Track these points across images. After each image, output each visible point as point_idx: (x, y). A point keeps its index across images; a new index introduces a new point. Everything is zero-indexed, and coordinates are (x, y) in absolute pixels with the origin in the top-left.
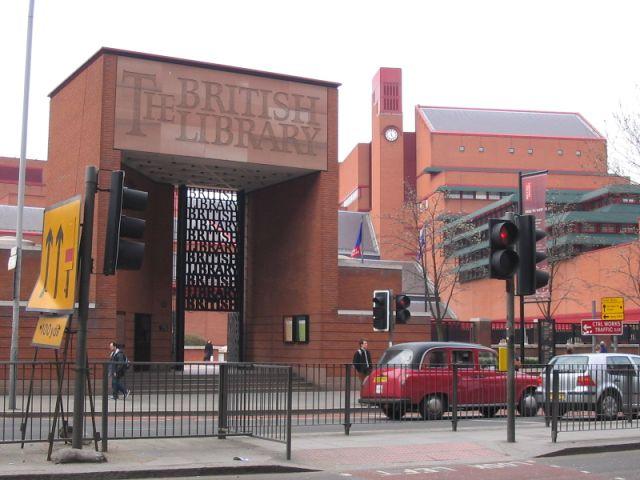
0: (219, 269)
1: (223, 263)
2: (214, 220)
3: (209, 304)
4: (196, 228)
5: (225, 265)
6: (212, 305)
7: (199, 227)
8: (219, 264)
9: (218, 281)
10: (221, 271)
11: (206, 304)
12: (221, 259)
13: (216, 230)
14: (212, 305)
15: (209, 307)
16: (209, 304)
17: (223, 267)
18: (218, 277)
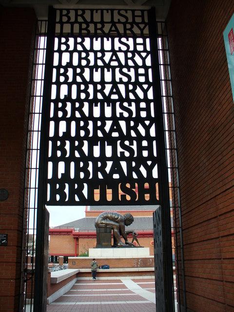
0: (116, 127)
1: (122, 117)
2: (103, 51)
3: (97, 192)
4: (68, 98)
5: (128, 121)
6: (103, 195)
7: (74, 96)
8: (115, 119)
9: (114, 150)
10: (119, 130)
11: (91, 193)
12: (119, 110)
13: (107, 66)
14: (103, 195)
15: (97, 198)
16: (97, 192)
17: (123, 124)
18: (113, 142)
